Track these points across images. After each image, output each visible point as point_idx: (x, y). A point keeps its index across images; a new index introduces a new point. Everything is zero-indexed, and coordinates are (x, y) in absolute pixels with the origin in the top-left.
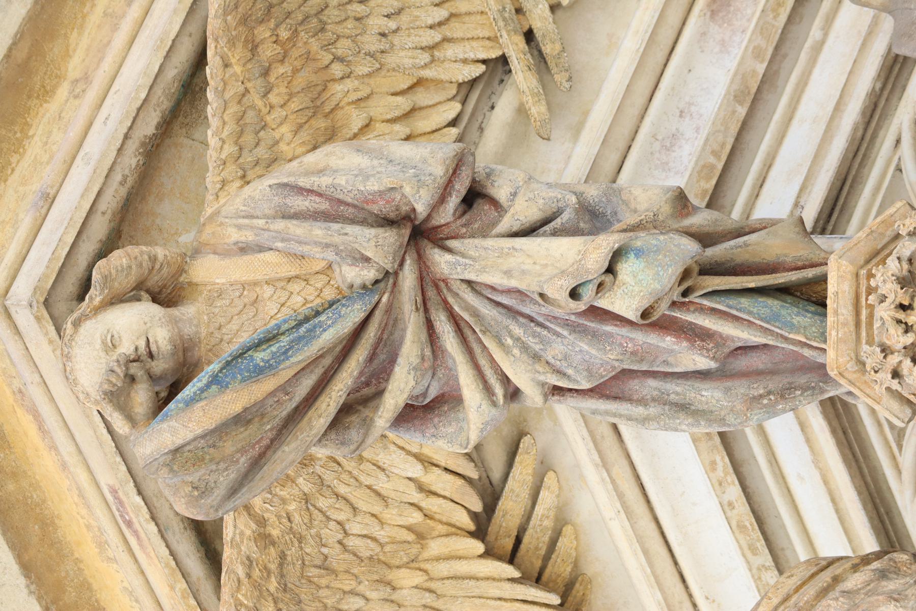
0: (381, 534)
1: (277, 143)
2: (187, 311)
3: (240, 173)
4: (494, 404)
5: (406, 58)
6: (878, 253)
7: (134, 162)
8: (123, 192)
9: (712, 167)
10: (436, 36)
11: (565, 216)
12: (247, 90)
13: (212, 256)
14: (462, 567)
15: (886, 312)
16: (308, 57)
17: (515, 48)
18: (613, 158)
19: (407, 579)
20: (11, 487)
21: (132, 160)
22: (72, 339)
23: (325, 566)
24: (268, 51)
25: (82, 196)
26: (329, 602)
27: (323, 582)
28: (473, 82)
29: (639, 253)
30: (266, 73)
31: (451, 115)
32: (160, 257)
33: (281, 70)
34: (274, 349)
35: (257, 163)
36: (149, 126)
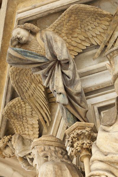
0: (36, 78)
1: (63, 29)
2: (33, 37)
3: (54, 29)
4: (47, 85)
5: (89, 34)
6: (83, 127)
7: (46, 14)
8: (41, 16)
9: (100, 87)
10: (95, 36)
11: (68, 79)
12: (64, 20)
13: (40, 35)
14: (40, 90)
15: (72, 135)
16: (77, 23)
17: (102, 46)
18: (97, 71)
19: (34, 85)
20: (9, 29)
21: (46, 14)
22: (16, 28)
23: (27, 75)
24: (72, 18)
25: (35, 13)
26: (23, 78)
27: (25, 76)
28: (93, 45)
29: (64, 96)
30: (69, 20)
31: (87, 46)
32: (35, 29)
33: (72, 22)
34: (30, 55)
35: (58, 29)
36: (52, 12)
